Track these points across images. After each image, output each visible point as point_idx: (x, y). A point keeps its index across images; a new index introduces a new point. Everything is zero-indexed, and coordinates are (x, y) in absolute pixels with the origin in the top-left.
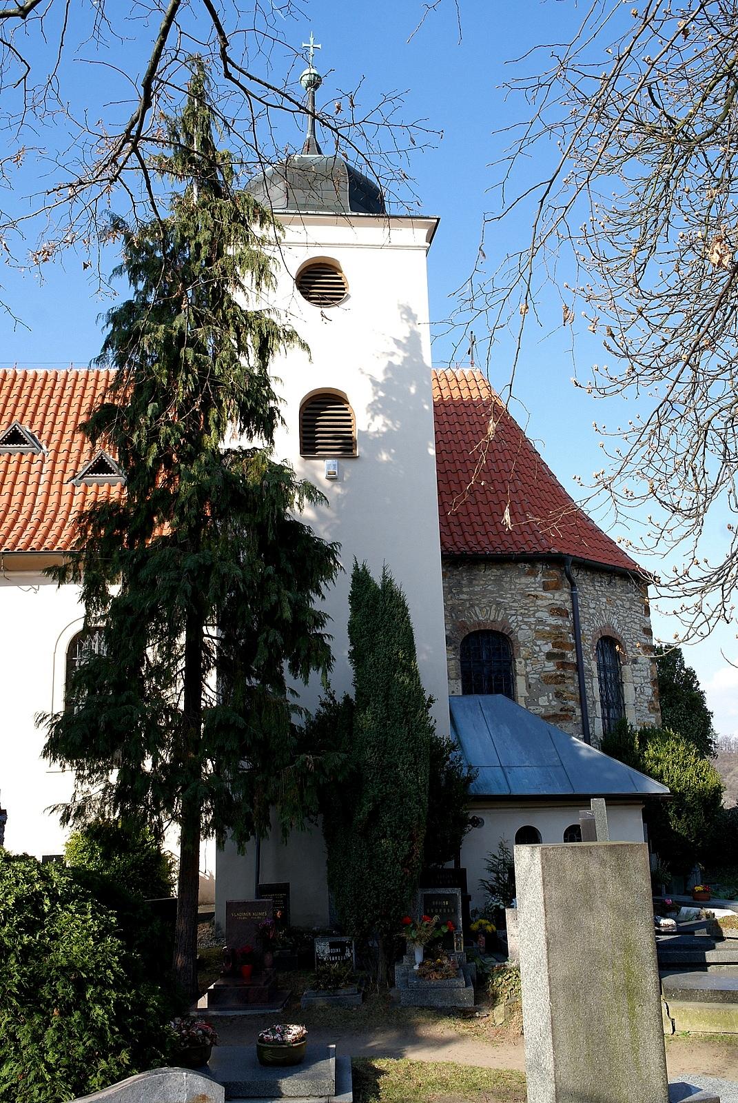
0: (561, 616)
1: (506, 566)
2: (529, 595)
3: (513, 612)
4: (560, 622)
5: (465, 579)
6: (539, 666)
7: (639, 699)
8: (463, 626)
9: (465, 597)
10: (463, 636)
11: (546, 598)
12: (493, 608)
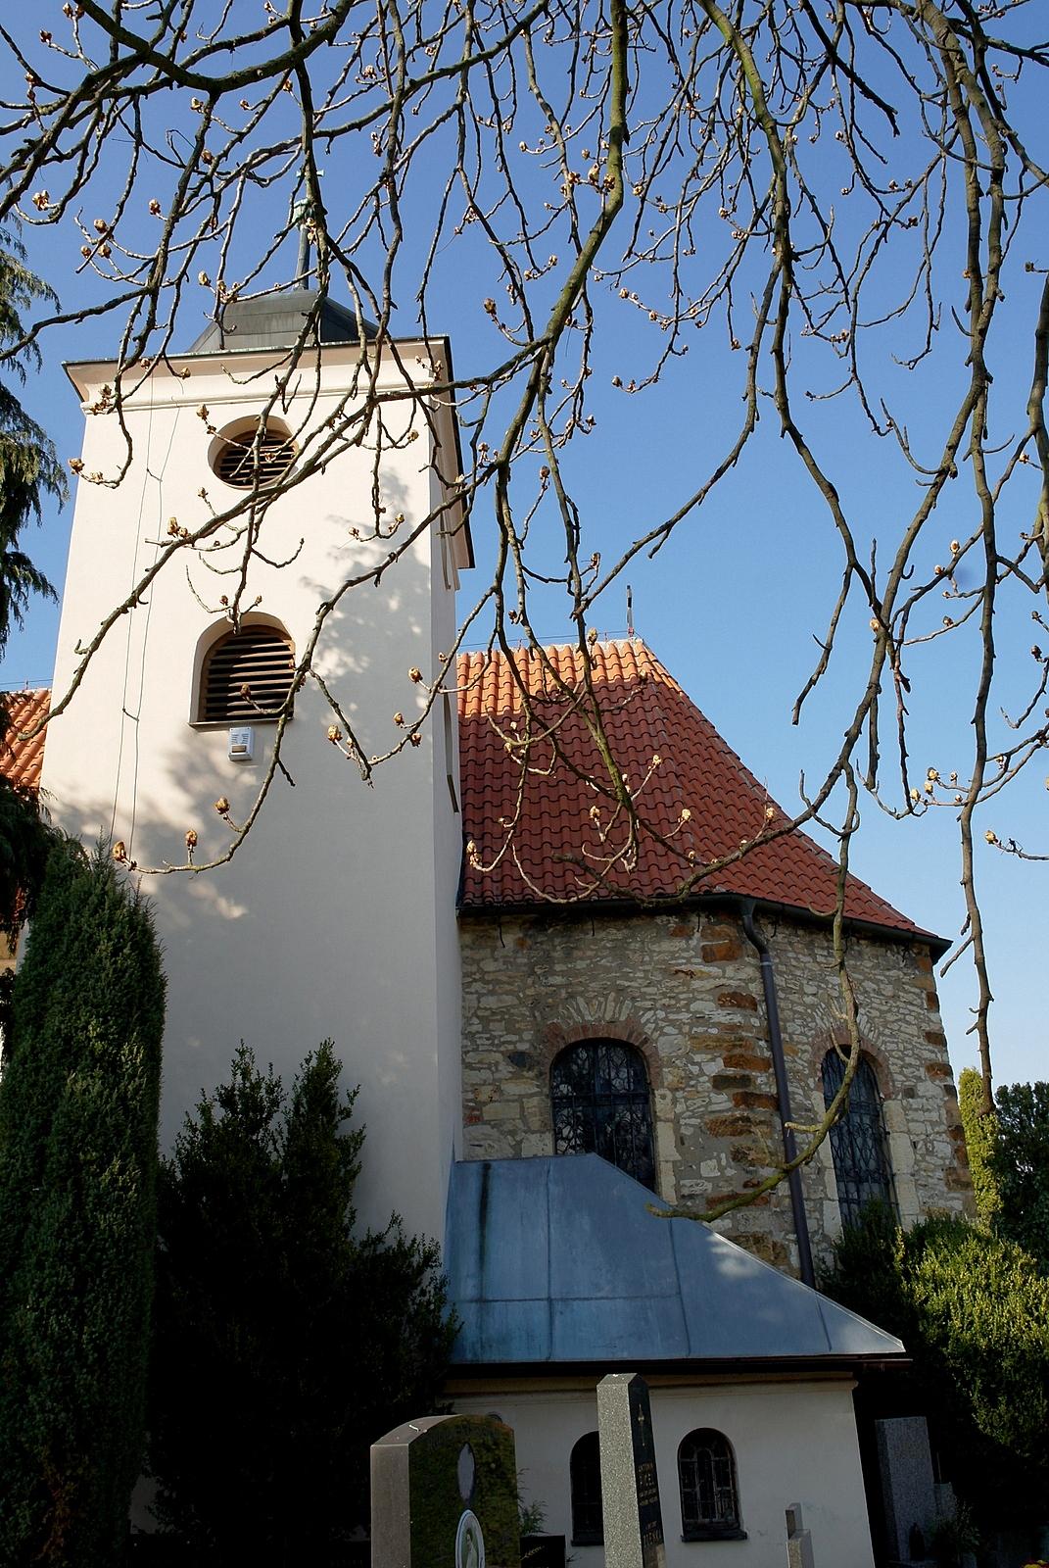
0: (739, 1006)
1: (635, 922)
2: (677, 972)
3: (648, 1004)
4: (737, 1019)
5: (558, 948)
6: (699, 1102)
7: (923, 1165)
8: (555, 1032)
9: (558, 980)
10: (555, 1050)
11: (709, 976)
12: (611, 998)
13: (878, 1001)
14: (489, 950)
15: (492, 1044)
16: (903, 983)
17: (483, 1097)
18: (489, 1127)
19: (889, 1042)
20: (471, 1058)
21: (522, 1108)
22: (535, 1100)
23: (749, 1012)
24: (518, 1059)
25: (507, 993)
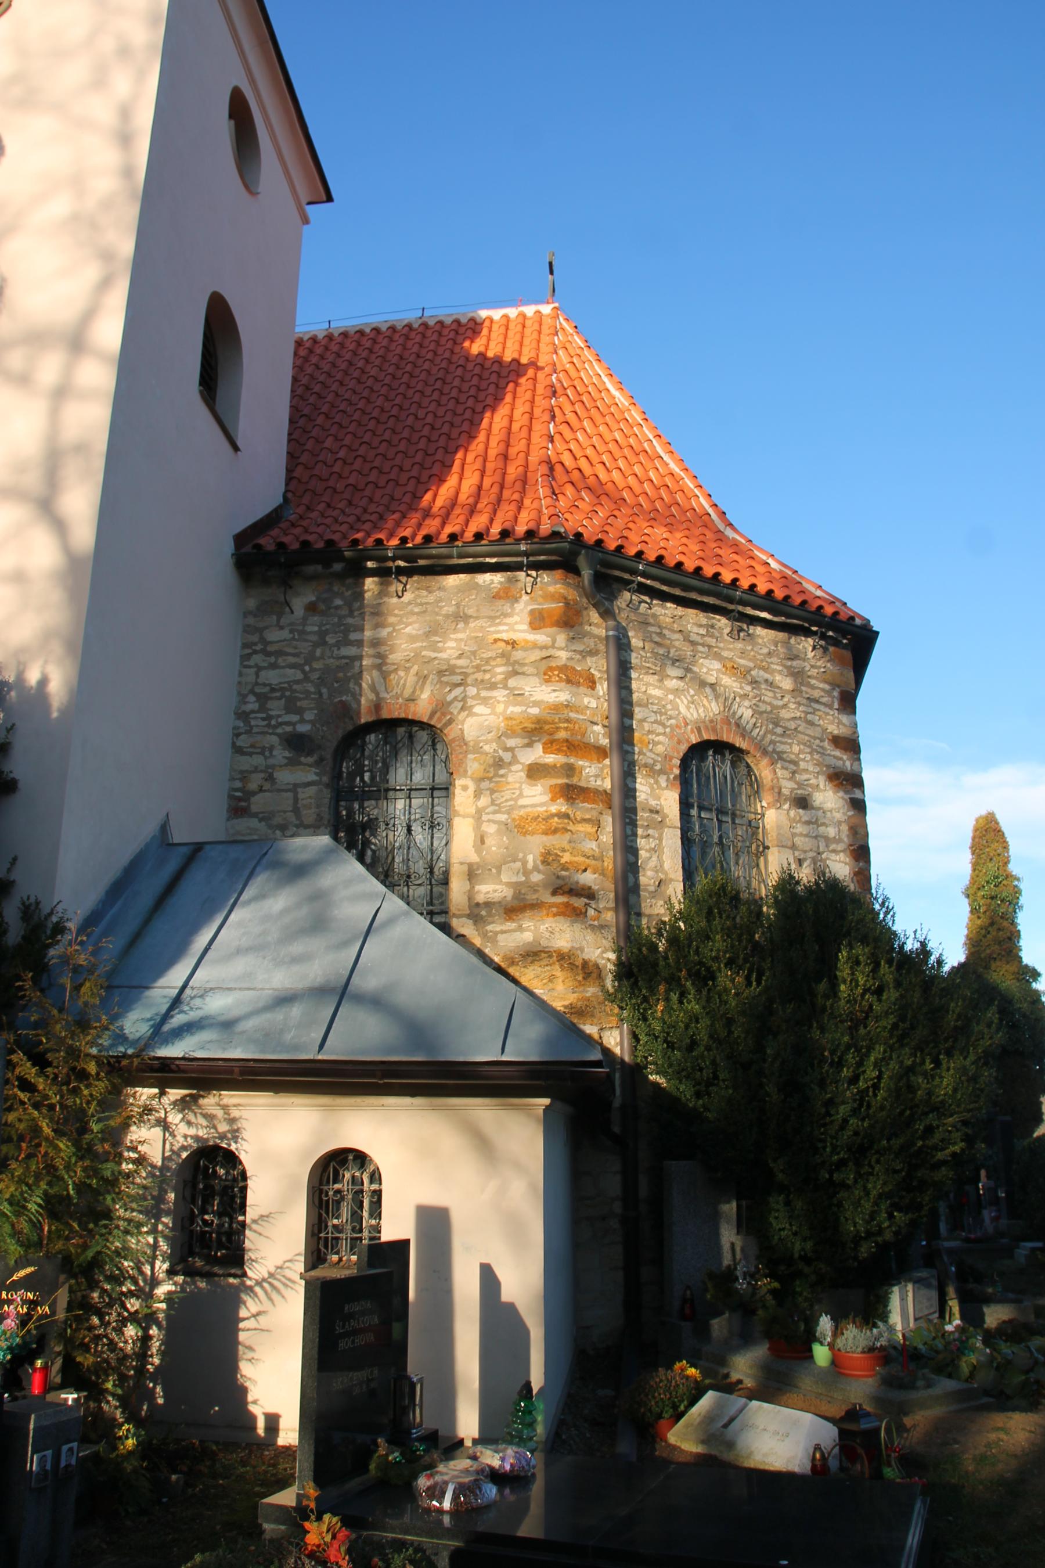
2: (496, 641)
3: (457, 679)
10: (340, 733)
13: (770, 694)
14: (275, 617)
15: (268, 726)
16: (809, 677)
17: (253, 786)
18: (256, 820)
19: (779, 742)
20: (243, 741)
21: (296, 800)
22: (312, 790)
23: (582, 689)
24: (298, 744)
25: (292, 666)
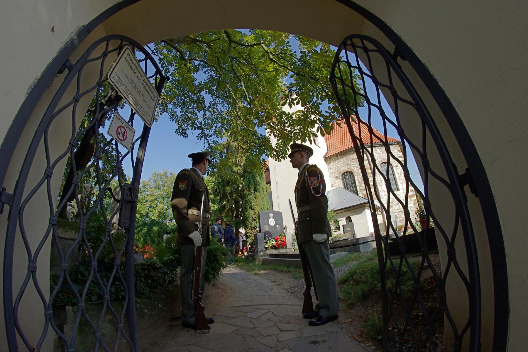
8: (340, 172)
20: (331, 179)
24: (337, 177)
